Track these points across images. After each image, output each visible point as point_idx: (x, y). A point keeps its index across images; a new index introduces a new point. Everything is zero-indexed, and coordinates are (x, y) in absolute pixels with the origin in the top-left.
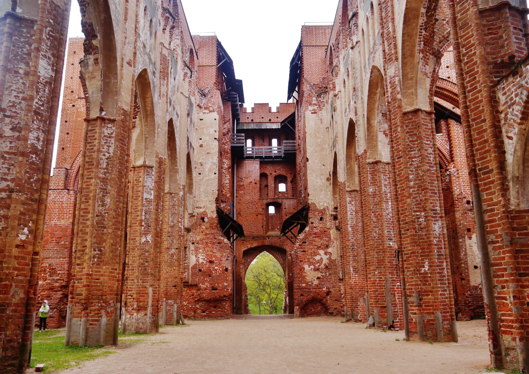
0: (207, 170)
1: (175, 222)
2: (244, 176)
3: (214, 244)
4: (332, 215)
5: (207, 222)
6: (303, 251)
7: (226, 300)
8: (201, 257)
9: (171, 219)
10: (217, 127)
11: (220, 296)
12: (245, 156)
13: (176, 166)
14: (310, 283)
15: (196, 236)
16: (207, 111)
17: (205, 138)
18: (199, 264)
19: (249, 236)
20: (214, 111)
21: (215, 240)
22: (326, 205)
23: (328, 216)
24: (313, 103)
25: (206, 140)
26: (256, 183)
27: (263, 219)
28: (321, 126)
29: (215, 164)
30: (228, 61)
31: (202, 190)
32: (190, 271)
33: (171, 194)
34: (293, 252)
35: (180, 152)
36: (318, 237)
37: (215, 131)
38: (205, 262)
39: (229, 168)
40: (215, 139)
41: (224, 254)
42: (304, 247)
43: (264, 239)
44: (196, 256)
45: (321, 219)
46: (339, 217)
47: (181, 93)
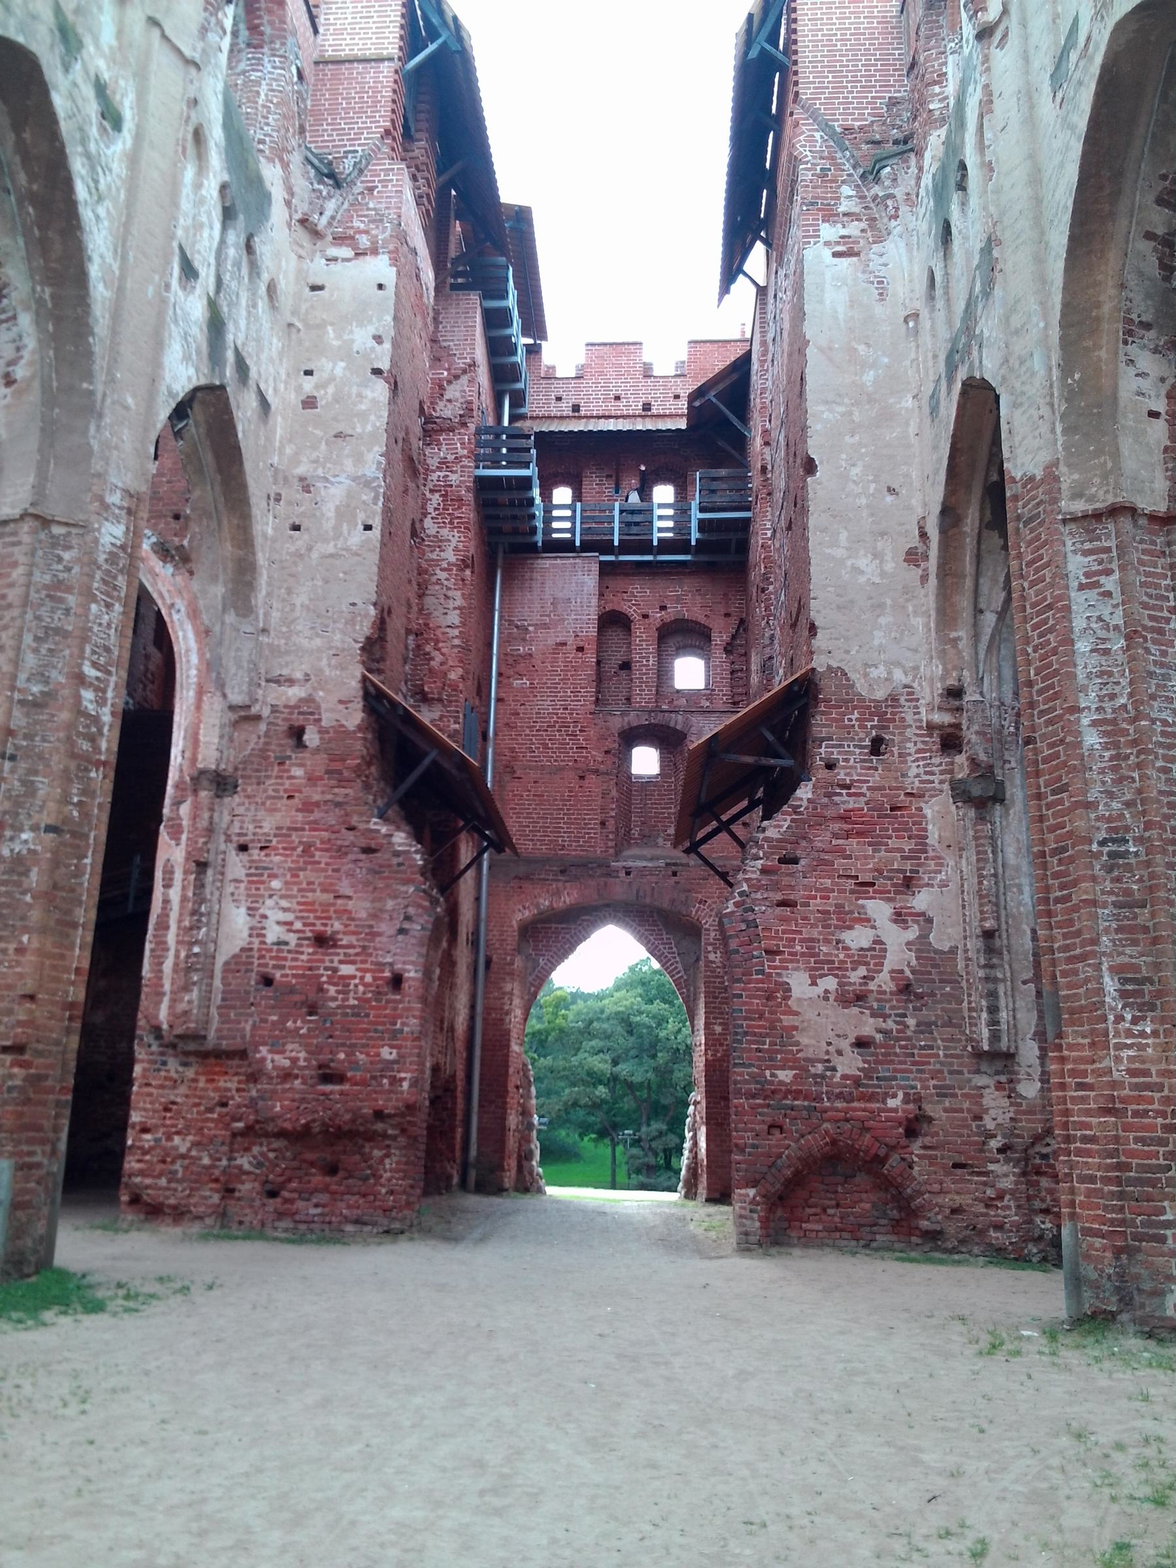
0: (329, 509)
1: (58, 677)
2: (536, 618)
3: (341, 852)
4: (931, 727)
5: (317, 750)
6: (783, 904)
7: (385, 1136)
8: (275, 915)
9: (30, 660)
10: (389, 318)
11: (356, 1113)
12: (539, 538)
13: (89, 376)
14: (820, 1068)
15: (261, 814)
16: (345, 252)
17: (332, 368)
18: (264, 950)
19: (545, 861)
20: (374, 251)
21: (350, 837)
22: (899, 676)
23: (909, 733)
24: (842, 209)
25: (332, 379)
26: (580, 649)
27: (604, 795)
28: (879, 310)
29: (367, 484)
30: (454, 46)
31: (301, 598)
32: (217, 983)
33: (45, 522)
34: (731, 907)
35: (116, 315)
36: (860, 834)
37: (378, 339)
38: (292, 939)
39: (464, 564)
40: (377, 372)
41: (390, 904)
42: (786, 880)
43: (608, 875)
44: (251, 911)
45: (877, 745)
46: (970, 734)
47: (153, 22)
